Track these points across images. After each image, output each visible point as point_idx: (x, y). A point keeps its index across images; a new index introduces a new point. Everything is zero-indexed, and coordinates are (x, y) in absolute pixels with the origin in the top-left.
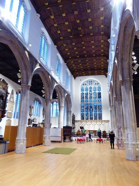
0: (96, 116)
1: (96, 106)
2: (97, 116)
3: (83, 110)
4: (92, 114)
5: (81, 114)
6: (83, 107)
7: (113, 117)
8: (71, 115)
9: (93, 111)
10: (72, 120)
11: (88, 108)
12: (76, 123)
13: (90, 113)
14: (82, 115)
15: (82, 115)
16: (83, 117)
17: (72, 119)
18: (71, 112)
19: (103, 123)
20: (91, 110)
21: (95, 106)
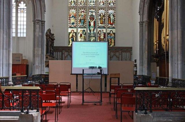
0: (102, 37)
1: (104, 16)
7: (177, 29)
8: (42, 32)
10: (47, 45)
13: (90, 31)
17: (47, 39)
18: (43, 22)
19: (117, 54)
20: (92, 24)
21: (100, 15)
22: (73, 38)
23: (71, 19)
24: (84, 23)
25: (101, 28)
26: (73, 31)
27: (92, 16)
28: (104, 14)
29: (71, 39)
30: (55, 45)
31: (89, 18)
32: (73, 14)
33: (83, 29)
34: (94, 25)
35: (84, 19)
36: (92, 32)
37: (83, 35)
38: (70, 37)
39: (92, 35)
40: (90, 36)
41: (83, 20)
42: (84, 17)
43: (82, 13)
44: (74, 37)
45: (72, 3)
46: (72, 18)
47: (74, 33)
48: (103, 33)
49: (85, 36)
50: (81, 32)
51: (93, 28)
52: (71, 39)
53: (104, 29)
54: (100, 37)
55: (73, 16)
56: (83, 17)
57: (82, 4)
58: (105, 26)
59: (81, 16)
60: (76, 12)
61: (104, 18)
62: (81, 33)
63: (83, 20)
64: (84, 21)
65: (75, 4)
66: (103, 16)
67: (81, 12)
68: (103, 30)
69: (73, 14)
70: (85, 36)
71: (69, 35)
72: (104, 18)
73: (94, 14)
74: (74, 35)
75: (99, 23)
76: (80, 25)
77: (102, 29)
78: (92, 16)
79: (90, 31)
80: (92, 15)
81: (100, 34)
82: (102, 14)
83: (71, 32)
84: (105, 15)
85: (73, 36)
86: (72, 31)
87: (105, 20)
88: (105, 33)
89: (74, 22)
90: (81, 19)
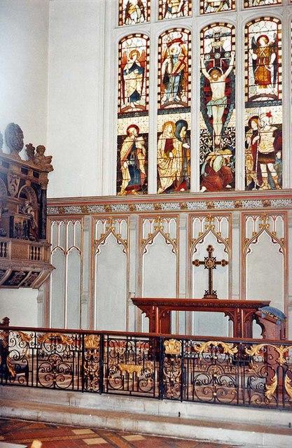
0: (266, 146)
1: (274, 47)
2: (278, 145)
3: (136, 96)
4: (229, 135)
5: (121, 140)
6: (141, 67)
9: (240, 99)
11: (184, 75)
12: (55, 230)
13: (209, 120)
14: (126, 147)
15: (126, 147)
16: (133, 170)
20: (218, 89)
21: (256, 47)
22: (137, 161)
23: (125, 77)
24: (180, 88)
25: (262, 104)
26: (137, 128)
27: (218, 56)
28: (272, 40)
29: (126, 165)
30: (51, 193)
31: (203, 66)
32: (135, 58)
33: (175, 117)
34: (226, 91)
35: (183, 72)
36: (217, 128)
37: (177, 144)
38: (122, 157)
39: (217, 141)
40: (210, 143)
41: (175, 75)
42: (182, 62)
43: (175, 46)
44: (140, 157)
45: (130, 12)
46: (132, 75)
47: (140, 135)
48: (272, 125)
49: (186, 145)
50: (170, 128)
51: (222, 110)
52: (126, 165)
53: (272, 109)
54: (255, 147)
55: (134, 66)
56: (177, 62)
57: (173, 11)
58: (280, 92)
59: (168, 60)
60: (148, 47)
61: (273, 57)
62: (169, 136)
63: (175, 75)
64: (180, 82)
65: (143, 12)
66: (270, 46)
67: (169, 45)
68: (269, 115)
69: (135, 58)
70: (186, 145)
71: (120, 147)
72: (273, 57)
73: (226, 44)
74: (139, 145)
75: (252, 81)
76: (164, 99)
77: (264, 110)
78: (218, 56)
79: (209, 120)
80: (217, 50)
81: (256, 133)
82: (262, 41)
83: (129, 135)
84: (280, 43)
85: (134, 148)
86: (132, 130)
87: (280, 65)
88: (279, 127)
89: (139, 89)
90: (166, 73)
